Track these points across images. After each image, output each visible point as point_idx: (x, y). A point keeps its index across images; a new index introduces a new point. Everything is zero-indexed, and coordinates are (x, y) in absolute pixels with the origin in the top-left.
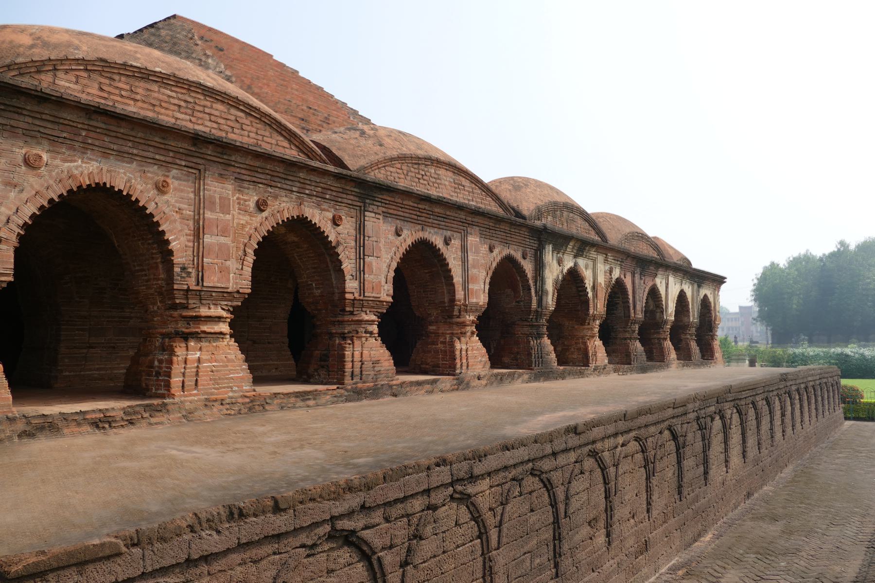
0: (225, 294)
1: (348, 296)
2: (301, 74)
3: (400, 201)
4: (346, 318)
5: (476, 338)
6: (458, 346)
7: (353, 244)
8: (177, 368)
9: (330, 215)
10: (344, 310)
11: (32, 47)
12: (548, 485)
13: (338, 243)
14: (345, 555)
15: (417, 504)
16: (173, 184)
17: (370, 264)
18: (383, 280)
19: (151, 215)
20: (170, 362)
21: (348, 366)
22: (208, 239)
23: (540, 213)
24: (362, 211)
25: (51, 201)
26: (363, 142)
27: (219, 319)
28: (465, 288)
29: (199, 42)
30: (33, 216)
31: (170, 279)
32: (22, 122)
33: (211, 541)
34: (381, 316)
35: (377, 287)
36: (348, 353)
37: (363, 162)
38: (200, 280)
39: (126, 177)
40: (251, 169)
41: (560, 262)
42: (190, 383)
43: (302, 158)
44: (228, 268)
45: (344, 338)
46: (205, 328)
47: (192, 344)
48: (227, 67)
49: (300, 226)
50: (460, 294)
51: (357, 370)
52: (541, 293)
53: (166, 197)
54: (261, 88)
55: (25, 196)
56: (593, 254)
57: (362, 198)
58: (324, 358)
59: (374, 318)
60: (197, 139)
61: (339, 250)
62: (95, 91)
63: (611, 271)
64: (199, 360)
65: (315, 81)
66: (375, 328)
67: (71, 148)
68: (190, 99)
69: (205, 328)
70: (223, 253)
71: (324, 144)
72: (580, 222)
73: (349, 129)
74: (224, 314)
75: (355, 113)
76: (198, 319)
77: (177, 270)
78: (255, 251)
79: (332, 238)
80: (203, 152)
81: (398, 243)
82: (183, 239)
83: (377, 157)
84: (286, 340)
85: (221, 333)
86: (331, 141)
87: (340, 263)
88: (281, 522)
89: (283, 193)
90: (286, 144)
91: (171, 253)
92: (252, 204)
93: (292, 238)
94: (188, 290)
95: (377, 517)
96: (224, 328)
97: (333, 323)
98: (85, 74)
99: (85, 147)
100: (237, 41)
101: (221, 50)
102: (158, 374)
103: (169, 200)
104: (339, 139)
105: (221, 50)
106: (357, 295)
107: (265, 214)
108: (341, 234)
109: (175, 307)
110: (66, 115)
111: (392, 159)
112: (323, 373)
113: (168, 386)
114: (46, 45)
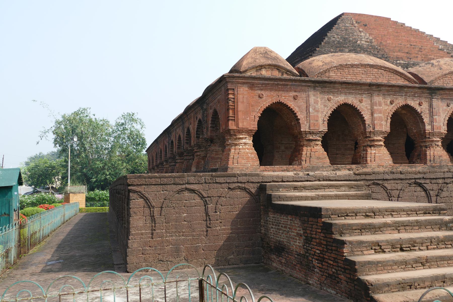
0: (382, 132)
1: (426, 131)
2: (406, 25)
3: (448, 92)
4: (427, 140)
7: (428, 112)
8: (369, 155)
9: (418, 103)
10: (426, 137)
11: (323, 66)
13: (422, 112)
14: (419, 189)
15: (440, 181)
16: (364, 99)
17: (436, 119)
18: (442, 125)
19: (359, 110)
20: (367, 154)
21: (428, 157)
22: (375, 115)
24: (431, 99)
25: (334, 109)
26: (432, 69)
27: (380, 140)
29: (356, 25)
30: (331, 114)
31: (365, 129)
32: (326, 90)
33: (387, 177)
34: (442, 138)
36: (428, 153)
37: (432, 78)
38: (374, 128)
39: (352, 100)
40: (388, 91)
42: (373, 160)
43: (406, 83)
44: (382, 124)
45: (427, 147)
46: (376, 143)
47: (372, 148)
48: (370, 34)
49: (407, 107)
51: (432, 159)
53: (362, 104)
54: (386, 41)
55: (328, 108)
57: (431, 94)
58: (419, 155)
59: (439, 139)
60: (370, 85)
61: (422, 115)
62: (339, 75)
64: (375, 153)
65: (414, 27)
66: (440, 144)
67: (338, 94)
68: (366, 70)
69: (376, 143)
70: (380, 119)
71: (415, 73)
73: (426, 64)
74: (382, 139)
75: (438, 40)
76: (374, 141)
77: (367, 126)
78: (391, 118)
79: (419, 110)
80: (373, 88)
81: (448, 110)
82: (368, 116)
83: (439, 75)
84: (405, 153)
85: (381, 145)
86: (418, 71)
87: (423, 119)
88: (402, 176)
89: (399, 97)
90: (399, 78)
91: (365, 121)
92: (389, 102)
93: (404, 112)
94: (370, 132)
95: (428, 181)
96: (382, 143)
97: (422, 142)
98: (336, 70)
100: (372, 16)
101: (366, 26)
102: (363, 158)
103: (362, 104)
104: (422, 70)
105: (366, 26)
106: (430, 131)
107: (393, 105)
108: (423, 108)
109: (367, 137)
110: (336, 85)
111: (445, 75)
112: (419, 160)
113: (366, 161)
114: (326, 64)
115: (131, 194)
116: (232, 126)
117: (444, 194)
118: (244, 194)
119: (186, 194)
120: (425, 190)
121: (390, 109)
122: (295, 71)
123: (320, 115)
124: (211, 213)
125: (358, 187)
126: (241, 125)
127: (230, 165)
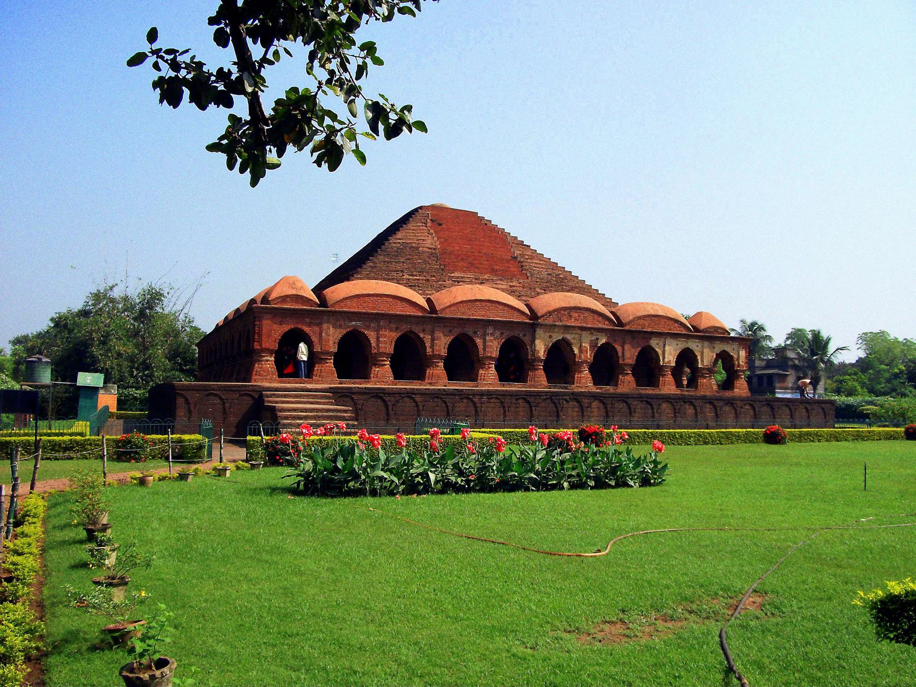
5: (493, 369)
6: (481, 371)
12: (445, 403)
23: (550, 313)
28: (484, 349)
35: (440, 350)
37: (442, 307)
41: (550, 337)
49: (411, 332)
50: (481, 352)
52: (534, 351)
56: (579, 332)
63: (597, 339)
70: (385, 342)
72: (587, 314)
99: (351, 321)
101: (440, 225)
105: (440, 225)
115: (178, 397)
116: (257, 346)
117: (399, 405)
118: (249, 398)
119: (213, 398)
120: (384, 401)
121: (395, 335)
122: (317, 301)
123: (331, 338)
124: (227, 409)
125: (326, 397)
126: (264, 346)
127: (254, 377)
